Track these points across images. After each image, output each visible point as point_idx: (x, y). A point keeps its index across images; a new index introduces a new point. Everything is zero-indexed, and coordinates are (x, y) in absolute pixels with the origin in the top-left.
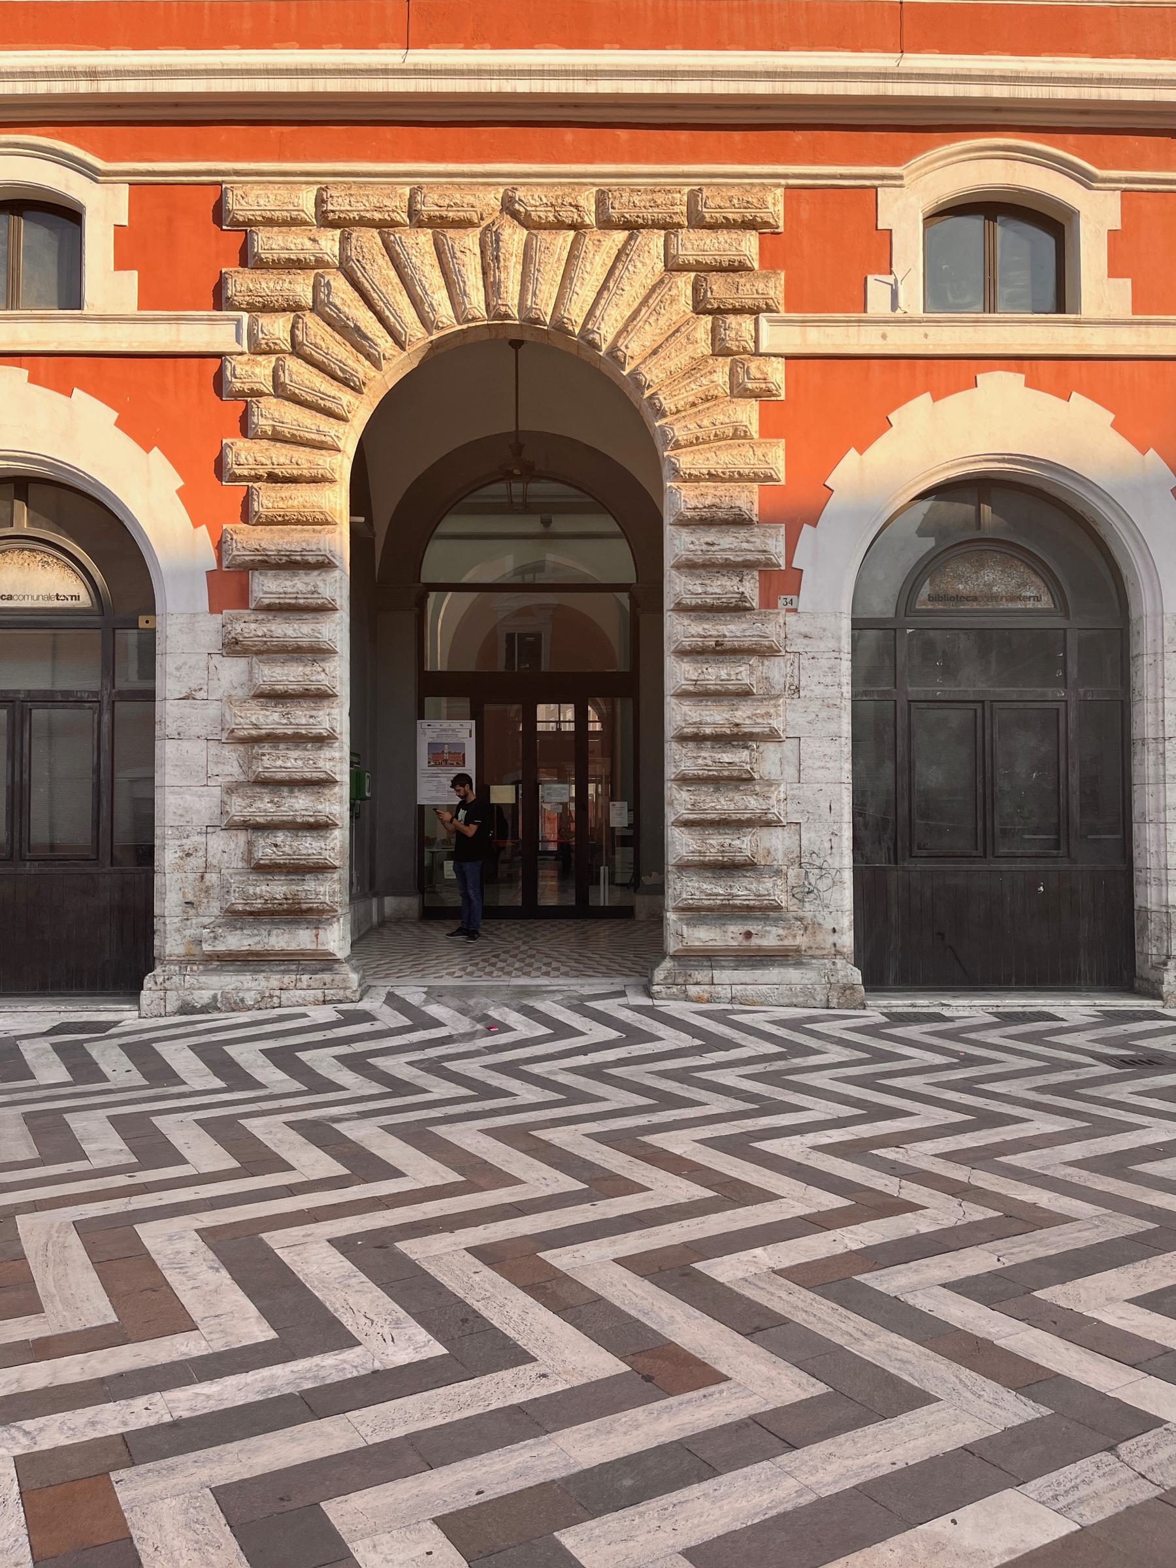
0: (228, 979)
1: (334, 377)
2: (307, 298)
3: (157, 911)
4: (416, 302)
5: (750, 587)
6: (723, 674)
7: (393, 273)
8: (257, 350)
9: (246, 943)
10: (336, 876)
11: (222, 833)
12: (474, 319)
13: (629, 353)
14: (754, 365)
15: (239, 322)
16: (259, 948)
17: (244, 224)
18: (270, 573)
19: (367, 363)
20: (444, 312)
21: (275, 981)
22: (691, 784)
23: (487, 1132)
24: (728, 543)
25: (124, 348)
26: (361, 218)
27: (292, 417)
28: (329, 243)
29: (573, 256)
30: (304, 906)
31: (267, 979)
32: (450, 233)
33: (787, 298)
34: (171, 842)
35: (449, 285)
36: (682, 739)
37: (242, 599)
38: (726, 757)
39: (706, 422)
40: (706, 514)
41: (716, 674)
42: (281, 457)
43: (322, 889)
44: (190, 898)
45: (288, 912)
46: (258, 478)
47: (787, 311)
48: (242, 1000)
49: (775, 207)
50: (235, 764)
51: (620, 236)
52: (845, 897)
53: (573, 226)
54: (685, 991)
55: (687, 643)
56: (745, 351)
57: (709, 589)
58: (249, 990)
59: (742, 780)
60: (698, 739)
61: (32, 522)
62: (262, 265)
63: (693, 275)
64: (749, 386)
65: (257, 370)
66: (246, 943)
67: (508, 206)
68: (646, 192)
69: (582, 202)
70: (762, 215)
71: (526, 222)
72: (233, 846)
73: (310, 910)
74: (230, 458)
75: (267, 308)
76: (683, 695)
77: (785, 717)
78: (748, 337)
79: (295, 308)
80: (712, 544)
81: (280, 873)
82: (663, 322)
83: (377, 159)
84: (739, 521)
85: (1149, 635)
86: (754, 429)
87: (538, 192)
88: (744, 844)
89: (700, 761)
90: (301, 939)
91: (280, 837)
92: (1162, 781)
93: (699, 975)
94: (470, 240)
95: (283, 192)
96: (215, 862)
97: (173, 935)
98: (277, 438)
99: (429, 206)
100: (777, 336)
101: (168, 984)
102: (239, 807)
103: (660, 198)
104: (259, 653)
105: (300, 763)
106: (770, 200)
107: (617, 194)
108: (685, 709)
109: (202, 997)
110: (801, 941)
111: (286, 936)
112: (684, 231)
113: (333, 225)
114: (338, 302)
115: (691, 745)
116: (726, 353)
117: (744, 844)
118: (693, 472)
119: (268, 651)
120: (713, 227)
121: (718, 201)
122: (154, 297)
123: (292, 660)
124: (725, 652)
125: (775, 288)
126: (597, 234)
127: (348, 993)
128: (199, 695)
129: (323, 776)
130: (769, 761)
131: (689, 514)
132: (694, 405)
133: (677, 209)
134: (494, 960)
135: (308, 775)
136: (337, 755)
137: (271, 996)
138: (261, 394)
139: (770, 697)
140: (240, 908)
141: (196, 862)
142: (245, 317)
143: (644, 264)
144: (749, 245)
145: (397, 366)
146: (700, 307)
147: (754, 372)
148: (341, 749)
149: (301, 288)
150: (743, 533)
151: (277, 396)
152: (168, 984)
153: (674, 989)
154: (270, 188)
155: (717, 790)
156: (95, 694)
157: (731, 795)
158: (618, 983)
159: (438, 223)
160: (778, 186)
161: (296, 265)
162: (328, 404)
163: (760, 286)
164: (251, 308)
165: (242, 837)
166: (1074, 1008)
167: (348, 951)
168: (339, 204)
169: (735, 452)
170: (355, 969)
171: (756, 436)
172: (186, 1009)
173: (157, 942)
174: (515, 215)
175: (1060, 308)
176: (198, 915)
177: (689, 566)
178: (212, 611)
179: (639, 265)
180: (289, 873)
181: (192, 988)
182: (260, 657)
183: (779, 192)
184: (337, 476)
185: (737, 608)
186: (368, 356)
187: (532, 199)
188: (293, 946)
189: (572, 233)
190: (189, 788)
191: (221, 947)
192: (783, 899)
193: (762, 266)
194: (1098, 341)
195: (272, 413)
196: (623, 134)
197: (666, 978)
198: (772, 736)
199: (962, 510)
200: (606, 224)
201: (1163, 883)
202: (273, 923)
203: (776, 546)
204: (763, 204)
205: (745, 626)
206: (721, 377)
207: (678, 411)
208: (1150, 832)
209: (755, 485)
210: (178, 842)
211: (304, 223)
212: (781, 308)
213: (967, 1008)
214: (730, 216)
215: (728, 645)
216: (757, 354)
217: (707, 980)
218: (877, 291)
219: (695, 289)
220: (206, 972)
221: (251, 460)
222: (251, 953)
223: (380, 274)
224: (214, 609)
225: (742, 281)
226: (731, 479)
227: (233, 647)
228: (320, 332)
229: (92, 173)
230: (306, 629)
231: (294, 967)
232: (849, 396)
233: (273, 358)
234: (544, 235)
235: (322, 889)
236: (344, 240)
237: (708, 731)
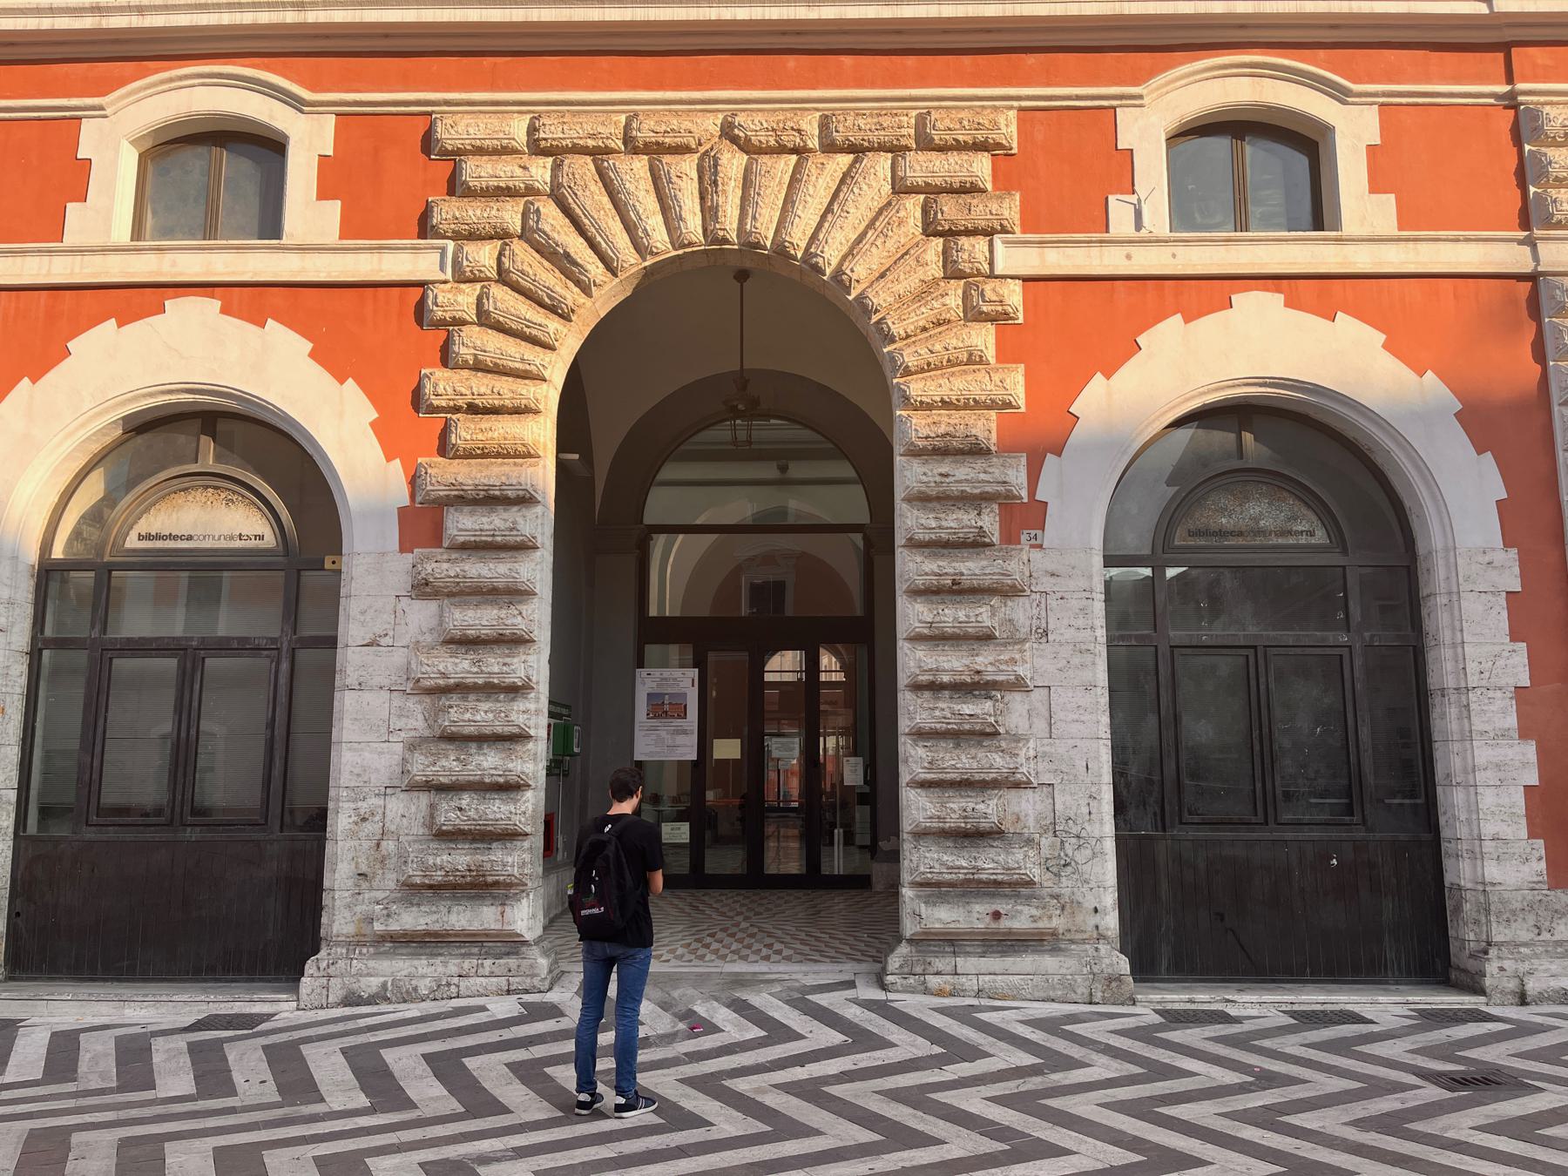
0: (401, 963)
1: (541, 304)
2: (515, 224)
3: (326, 884)
4: (630, 228)
5: (989, 521)
6: (961, 615)
7: (606, 199)
8: (461, 277)
9: (422, 921)
10: (526, 844)
11: (403, 796)
12: (690, 244)
13: (854, 277)
14: (989, 288)
15: (443, 250)
16: (437, 927)
17: (453, 153)
18: (466, 509)
19: (576, 290)
20: (659, 237)
21: (453, 966)
22: (928, 739)
24: (964, 474)
25: (323, 277)
26: (574, 145)
27: (494, 345)
28: (540, 171)
29: (795, 180)
30: (490, 879)
31: (445, 964)
32: (666, 159)
33: (1022, 220)
34: (346, 805)
35: (665, 210)
36: (917, 687)
37: (435, 536)
38: (967, 709)
39: (938, 347)
40: (938, 443)
41: (953, 615)
42: (482, 387)
43: (510, 859)
44: (364, 869)
45: (473, 886)
46: (457, 409)
47: (1024, 231)
48: (415, 989)
49: (1008, 129)
50: (420, 717)
51: (845, 160)
52: (1107, 871)
53: (795, 151)
54: (924, 982)
55: (920, 582)
56: (979, 274)
57: (944, 523)
58: (423, 976)
59: (985, 735)
60: (935, 687)
61: (218, 458)
62: (470, 193)
63: (922, 197)
64: (984, 309)
65: (460, 298)
66: (422, 921)
67: (728, 132)
68: (871, 115)
69: (804, 126)
70: (994, 136)
71: (746, 147)
72: (413, 809)
73: (496, 884)
74: (428, 388)
75: (474, 236)
76: (917, 638)
77: (1032, 663)
78: (982, 259)
79: (503, 235)
80: (947, 476)
81: (465, 840)
82: (891, 244)
83: (593, 88)
84: (976, 451)
85: (1441, 572)
86: (990, 354)
87: (759, 117)
88: (989, 809)
89: (937, 713)
90: (484, 917)
91: (466, 800)
92: (1468, 737)
93: (940, 963)
95: (494, 122)
96: (393, 828)
97: (341, 914)
98: (479, 367)
99: (644, 134)
100: (1013, 258)
101: (331, 970)
102: (421, 766)
103: (886, 121)
104: (451, 595)
105: (491, 716)
106: (1002, 122)
107: (841, 118)
108: (920, 654)
109: (371, 985)
110: (1058, 922)
111: (468, 913)
112: (910, 156)
113: (545, 153)
114: (547, 228)
115: (927, 694)
116: (959, 275)
117: (989, 809)
118: (924, 399)
119: (461, 593)
120: (943, 149)
121: (947, 123)
122: (357, 227)
123: (485, 602)
124: (961, 592)
125: (1010, 209)
126: (821, 158)
127: (536, 981)
128: (383, 641)
129: (516, 730)
130: (1016, 713)
131: (920, 444)
132: (924, 329)
133: (904, 132)
134: (709, 940)
135: (499, 730)
136: (532, 707)
137: (449, 985)
138: (464, 323)
139: (1015, 641)
140: (418, 880)
141: (371, 828)
142: (450, 245)
143: (870, 186)
144: (981, 167)
145: (608, 294)
146: (930, 229)
147: (989, 295)
148: (537, 700)
149: (510, 215)
150: (980, 464)
151: (480, 324)
152: (331, 970)
153: (911, 980)
154: (479, 117)
155: (957, 746)
156: (273, 640)
157: (973, 751)
158: (846, 970)
159: (655, 150)
160: (1011, 108)
162: (534, 332)
163: (994, 207)
164: (457, 236)
165: (424, 799)
166: (1384, 1006)
167: (539, 931)
168: (552, 131)
169: (970, 378)
170: (545, 953)
171: (992, 361)
172: (351, 1000)
173: (324, 920)
174: (734, 140)
175: (1318, 224)
176: (371, 889)
177: (922, 499)
178: (402, 550)
179: (865, 187)
180: (474, 840)
181: (360, 974)
182: (452, 600)
183: (1012, 114)
184: (541, 407)
185: (976, 544)
186: (578, 283)
187: (753, 124)
188: (475, 926)
189: (794, 158)
190: (369, 745)
191: (394, 927)
192: (1035, 873)
193: (995, 188)
194: (1361, 259)
195: (474, 341)
196: (847, 60)
197: (901, 966)
198: (1018, 685)
199: (1221, 439)
200: (830, 148)
201: (1477, 856)
202: (454, 898)
203: (1017, 477)
204: (996, 125)
205: (984, 563)
206: (953, 298)
207: (908, 337)
208: (1458, 796)
209: (993, 414)
210: (353, 806)
211: (514, 151)
212: (1017, 229)
213: (1258, 1005)
214: (961, 138)
215: (966, 583)
216: (992, 276)
217: (949, 969)
218: (1120, 211)
219: (925, 211)
220: (377, 955)
221: (450, 390)
222: (428, 933)
223: (593, 200)
224: (405, 547)
225: (975, 202)
226: (966, 407)
227: (423, 589)
228: (528, 259)
229: (297, 104)
230: (502, 568)
231: (476, 950)
232: (1094, 320)
233: (478, 286)
234: (764, 159)
235: (510, 859)
236: (557, 167)
237: (946, 679)
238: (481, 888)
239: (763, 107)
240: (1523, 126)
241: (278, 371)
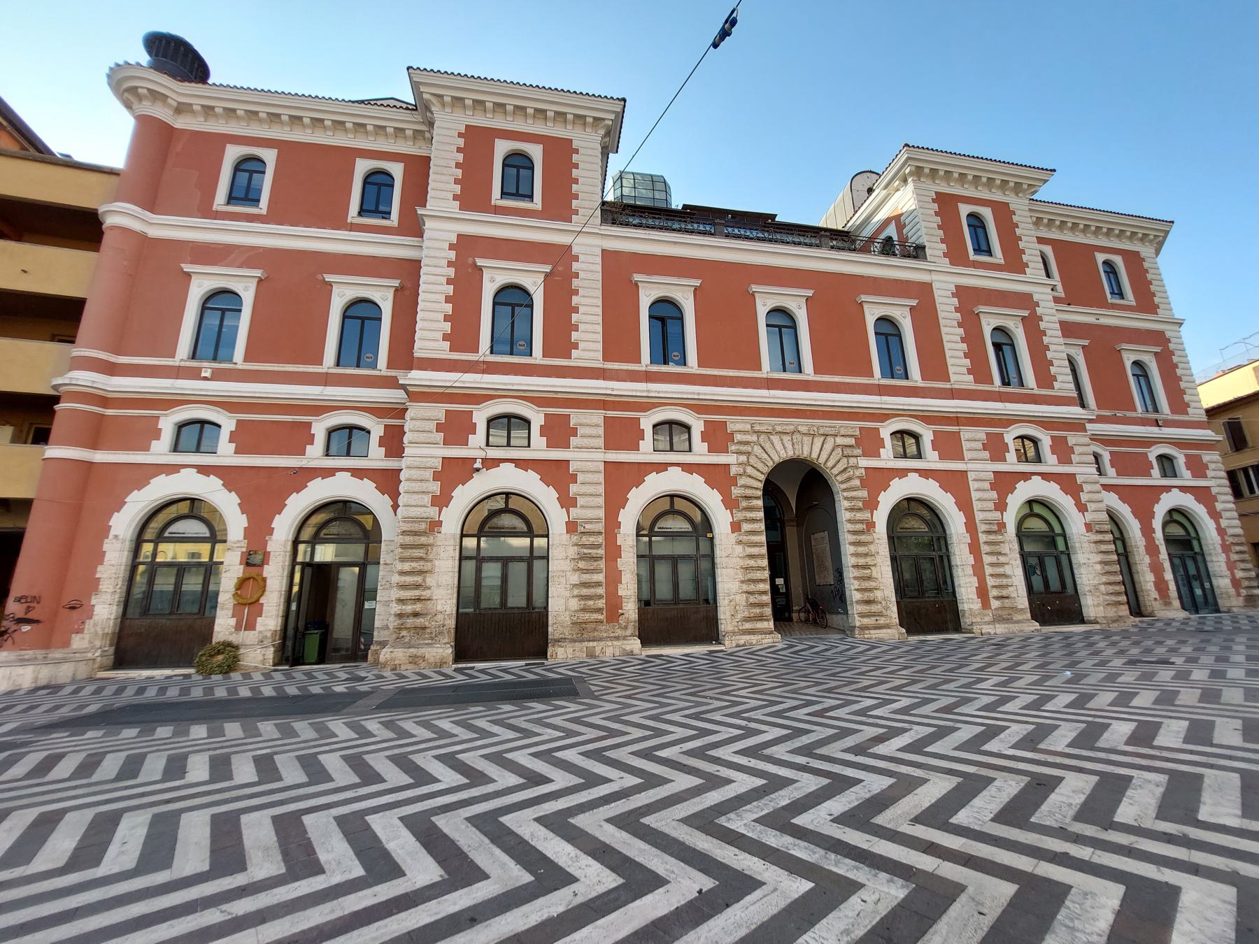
28: (754, 438)
42: (749, 492)
52: (895, 609)
59: (869, 578)
109: (742, 642)
168: (757, 428)
172: (738, 646)
187: (800, 428)
227: (740, 542)
238: (761, 618)
241: (696, 486)
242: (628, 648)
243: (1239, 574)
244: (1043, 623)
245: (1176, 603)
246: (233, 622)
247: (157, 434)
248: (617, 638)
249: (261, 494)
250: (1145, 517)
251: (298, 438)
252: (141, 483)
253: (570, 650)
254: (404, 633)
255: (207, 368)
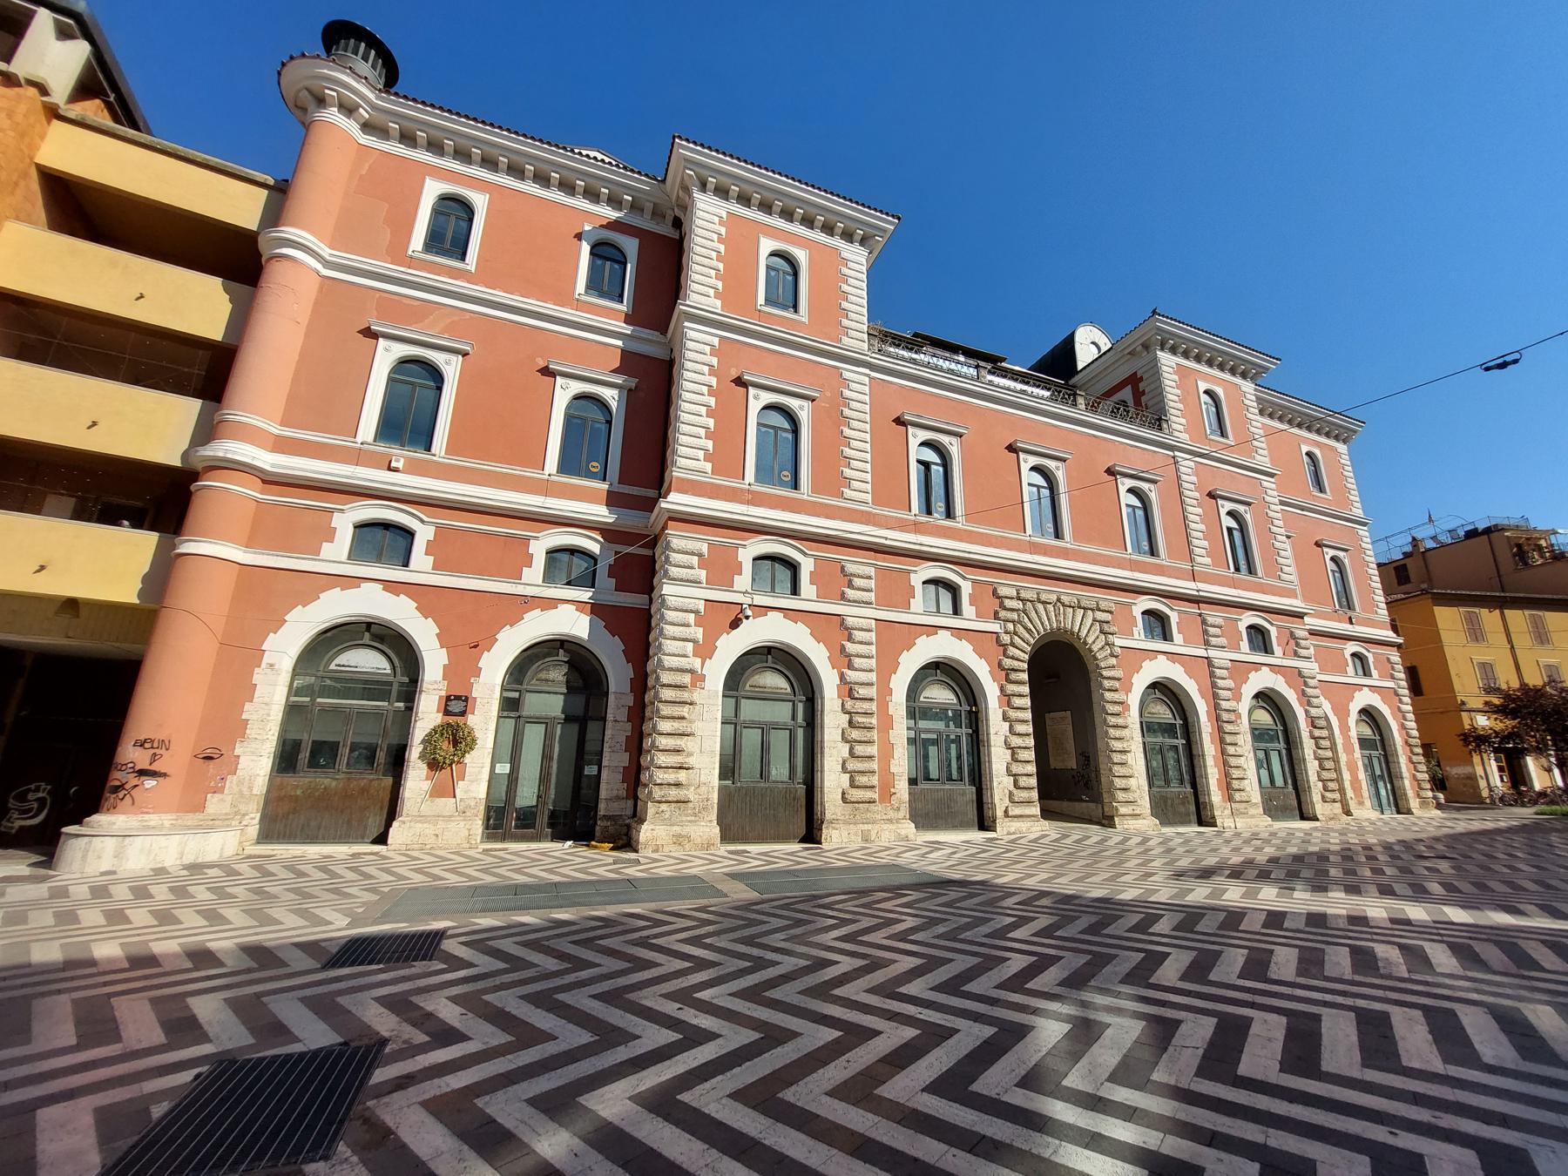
23: (573, 942)
67: (1059, 600)
94: (1050, 607)
100: (1118, 642)
154: (1007, 586)
159: (1044, 603)
161: (1013, 610)
187: (1065, 599)
223: (1033, 615)
239: (1069, 593)
240: (1204, 622)
242: (903, 832)
243: (1420, 776)
244: (1274, 818)
245: (1368, 803)
246: (427, 785)
247: (330, 535)
248: (890, 821)
249: (469, 624)
250: (1343, 713)
251: (512, 559)
252: (308, 598)
253: (845, 834)
254: (664, 807)
255: (400, 456)
